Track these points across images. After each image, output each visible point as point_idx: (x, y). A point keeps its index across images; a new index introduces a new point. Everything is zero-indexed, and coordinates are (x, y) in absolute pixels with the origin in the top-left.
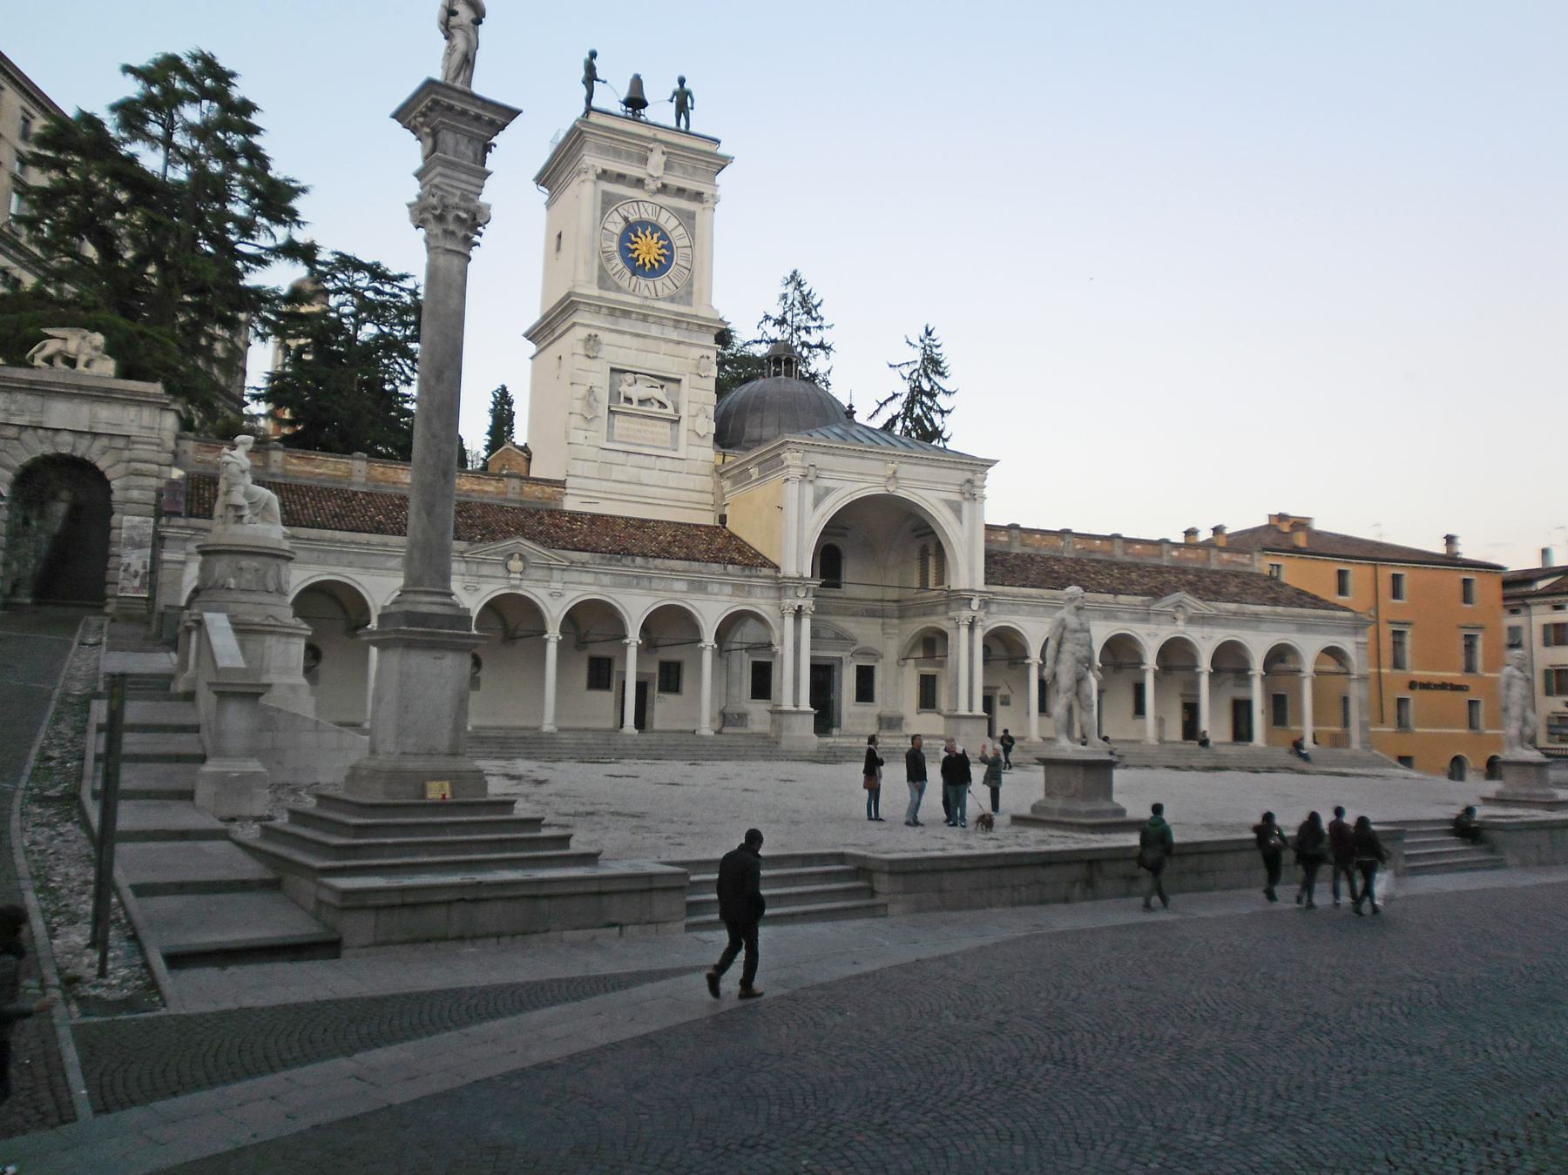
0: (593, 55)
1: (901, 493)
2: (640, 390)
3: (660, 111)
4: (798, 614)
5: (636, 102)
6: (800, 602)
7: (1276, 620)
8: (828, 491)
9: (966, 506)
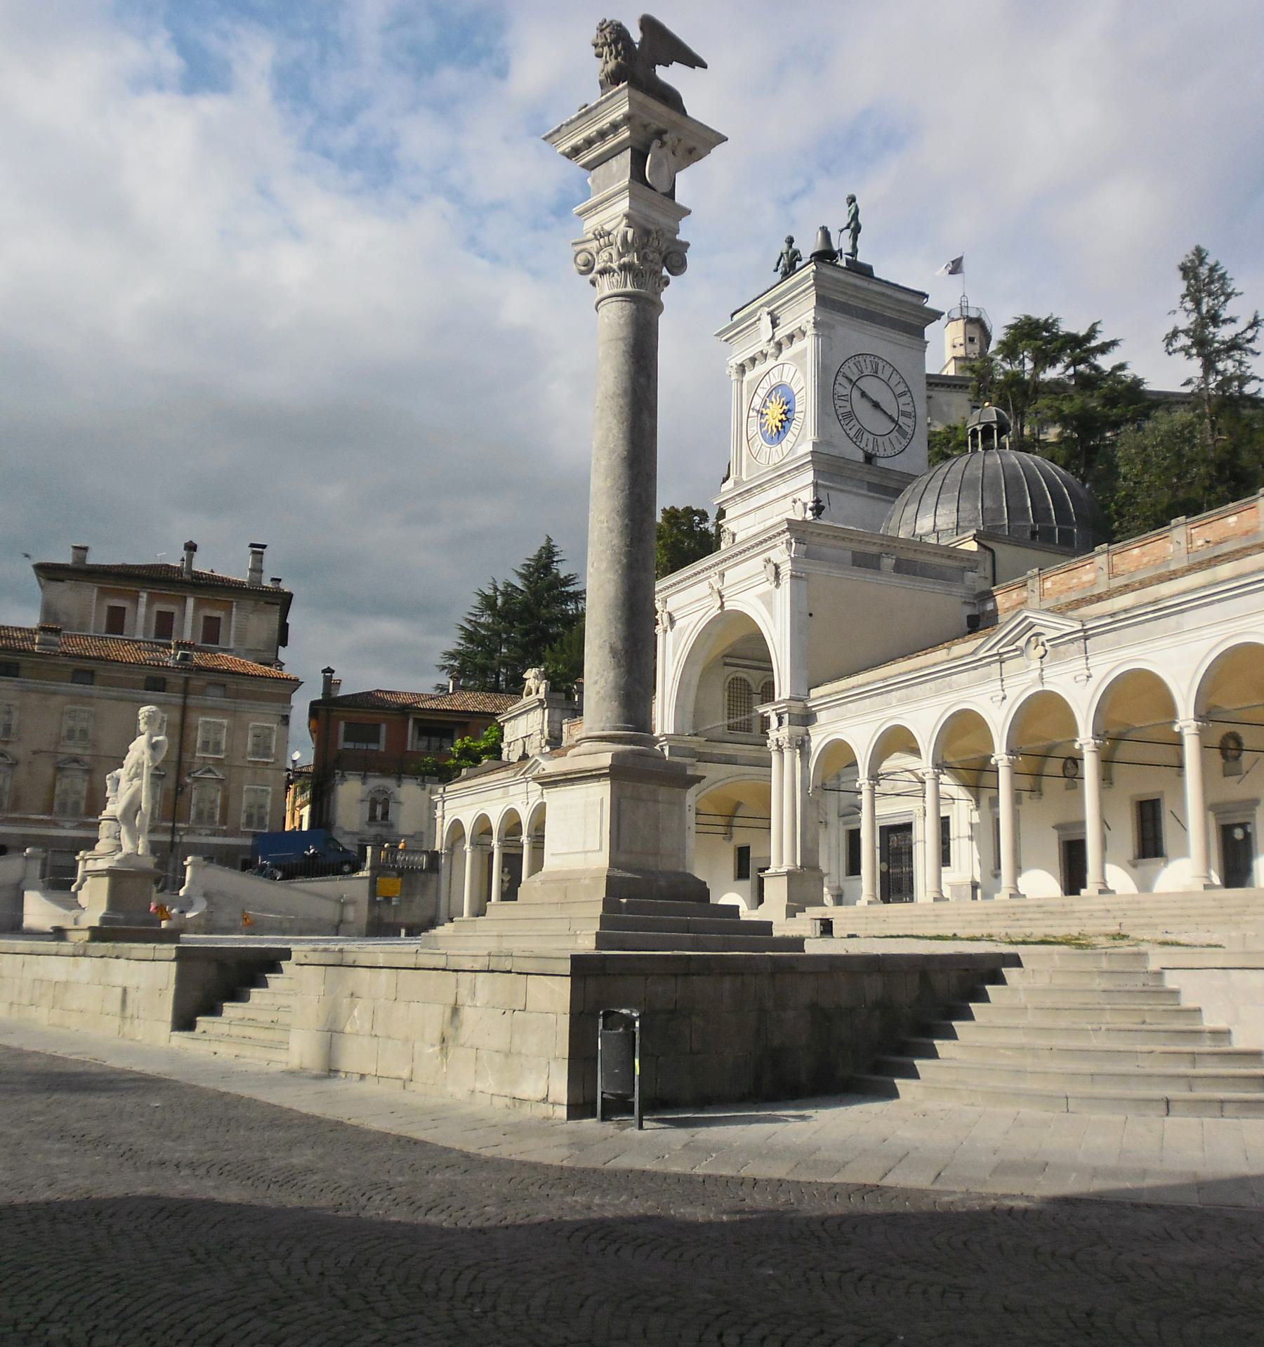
0: (790, 241)
1: (728, 606)
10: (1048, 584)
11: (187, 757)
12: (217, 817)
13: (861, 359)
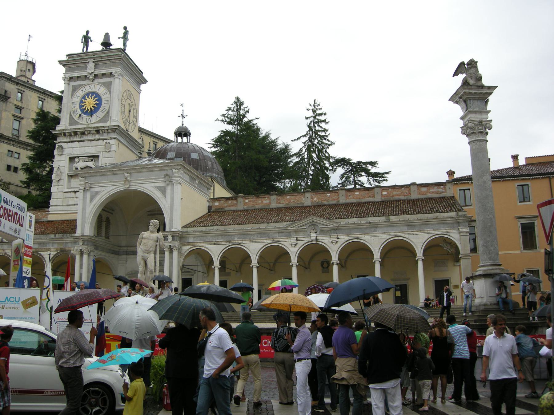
0: (88, 32)
1: (134, 187)
2: (80, 164)
3: (116, 44)
4: (82, 253)
5: (106, 44)
6: (81, 248)
7: (389, 225)
8: (97, 193)
9: (169, 189)
10: (247, 201)
13: (127, 91)
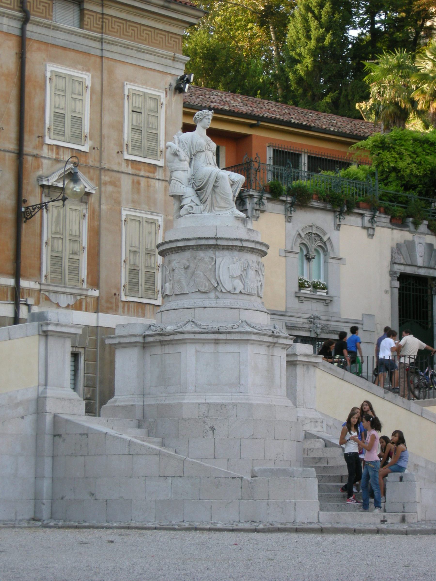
11: (29, 148)
12: (84, 273)
